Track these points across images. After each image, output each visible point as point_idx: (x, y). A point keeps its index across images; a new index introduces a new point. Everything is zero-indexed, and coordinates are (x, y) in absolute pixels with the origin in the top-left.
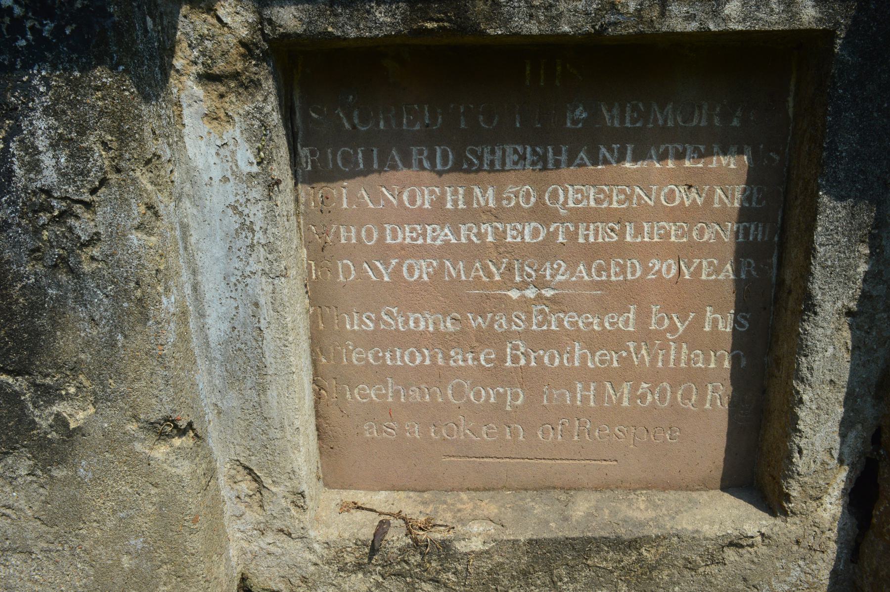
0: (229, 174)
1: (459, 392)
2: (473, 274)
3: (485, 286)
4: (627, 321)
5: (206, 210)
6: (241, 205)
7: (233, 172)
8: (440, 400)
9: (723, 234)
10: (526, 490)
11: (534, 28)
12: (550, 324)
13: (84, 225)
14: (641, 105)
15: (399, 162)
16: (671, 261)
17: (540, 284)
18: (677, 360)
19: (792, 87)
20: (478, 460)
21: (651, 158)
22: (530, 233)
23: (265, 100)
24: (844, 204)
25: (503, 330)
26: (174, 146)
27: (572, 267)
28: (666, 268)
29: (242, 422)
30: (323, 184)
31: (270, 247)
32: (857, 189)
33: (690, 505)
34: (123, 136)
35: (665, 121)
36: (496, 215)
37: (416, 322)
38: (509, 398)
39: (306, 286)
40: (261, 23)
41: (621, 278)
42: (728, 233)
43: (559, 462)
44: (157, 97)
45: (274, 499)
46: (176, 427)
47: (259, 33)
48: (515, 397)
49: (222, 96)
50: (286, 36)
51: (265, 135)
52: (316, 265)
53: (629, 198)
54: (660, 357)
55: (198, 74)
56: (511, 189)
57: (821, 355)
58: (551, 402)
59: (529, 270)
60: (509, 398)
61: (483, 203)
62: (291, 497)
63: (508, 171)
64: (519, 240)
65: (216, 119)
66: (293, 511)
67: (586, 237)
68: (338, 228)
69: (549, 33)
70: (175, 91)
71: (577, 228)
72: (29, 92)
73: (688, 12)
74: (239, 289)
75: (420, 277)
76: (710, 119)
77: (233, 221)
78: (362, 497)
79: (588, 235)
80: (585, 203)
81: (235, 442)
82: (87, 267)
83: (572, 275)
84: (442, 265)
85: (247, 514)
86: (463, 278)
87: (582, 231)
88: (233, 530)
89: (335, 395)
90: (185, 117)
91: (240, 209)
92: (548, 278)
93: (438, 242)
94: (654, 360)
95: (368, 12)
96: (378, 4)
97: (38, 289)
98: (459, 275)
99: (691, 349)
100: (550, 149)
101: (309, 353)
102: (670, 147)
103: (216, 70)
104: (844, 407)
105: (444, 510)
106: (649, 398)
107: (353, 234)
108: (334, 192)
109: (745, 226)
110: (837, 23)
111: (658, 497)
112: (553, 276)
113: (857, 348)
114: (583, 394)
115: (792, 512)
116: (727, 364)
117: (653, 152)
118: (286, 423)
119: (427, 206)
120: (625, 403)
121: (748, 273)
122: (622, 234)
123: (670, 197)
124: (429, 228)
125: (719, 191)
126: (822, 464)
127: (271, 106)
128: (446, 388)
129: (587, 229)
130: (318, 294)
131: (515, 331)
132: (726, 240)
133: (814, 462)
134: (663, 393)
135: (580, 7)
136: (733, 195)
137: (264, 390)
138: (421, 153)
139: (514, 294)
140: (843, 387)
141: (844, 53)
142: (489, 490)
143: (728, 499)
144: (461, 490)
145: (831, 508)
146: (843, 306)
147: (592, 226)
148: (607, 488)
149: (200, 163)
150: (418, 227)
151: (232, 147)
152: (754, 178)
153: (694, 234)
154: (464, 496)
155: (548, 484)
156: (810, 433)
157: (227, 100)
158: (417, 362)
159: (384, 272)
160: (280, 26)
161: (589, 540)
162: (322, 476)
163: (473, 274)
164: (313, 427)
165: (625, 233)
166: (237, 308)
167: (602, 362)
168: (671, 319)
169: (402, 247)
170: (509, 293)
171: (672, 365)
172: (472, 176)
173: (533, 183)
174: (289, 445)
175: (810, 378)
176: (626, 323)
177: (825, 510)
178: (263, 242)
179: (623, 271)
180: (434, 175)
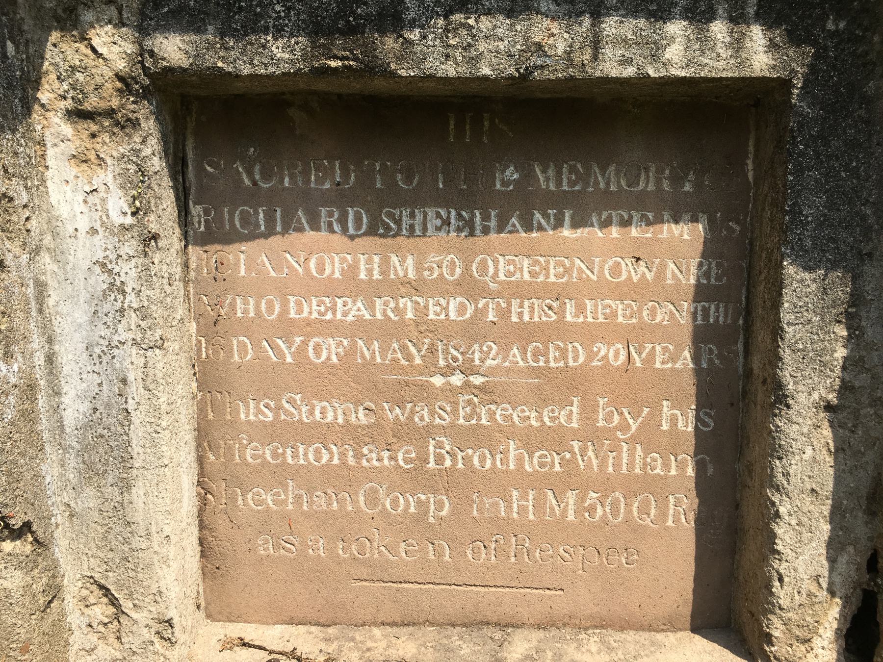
0: (97, 226)
1: (372, 499)
2: (389, 356)
3: (403, 371)
4: (570, 416)
5: (68, 267)
6: (111, 262)
7: (103, 224)
8: (350, 508)
9: (678, 316)
10: (454, 625)
11: (450, 70)
12: (479, 419)
14: (579, 166)
15: (305, 225)
16: (619, 346)
17: (468, 370)
18: (631, 464)
19: (751, 149)
20: (395, 585)
21: (592, 225)
22: (455, 308)
23: (144, 142)
24: (813, 276)
25: (425, 423)
26: (34, 190)
27: (505, 350)
29: (99, 528)
30: (218, 247)
31: (143, 312)
32: (828, 260)
33: (652, 649)
35: (608, 184)
36: (416, 288)
37: (323, 412)
38: (432, 507)
39: (194, 366)
40: (141, 55)
41: (562, 364)
42: (684, 314)
43: (493, 589)
44: (14, 131)
45: (134, 629)
46: (7, 526)
47: (139, 66)
48: (440, 506)
49: (93, 136)
50: (169, 70)
51: (143, 182)
52: (207, 342)
53: (568, 271)
54: (611, 461)
55: (67, 110)
56: (433, 258)
57: (797, 458)
58: (482, 513)
59: (455, 353)
60: (432, 507)
61: (401, 274)
62: (156, 627)
63: (429, 237)
64: (443, 317)
65: (85, 161)
66: (158, 645)
67: (520, 315)
68: (234, 299)
69: (468, 75)
70: (39, 127)
71: (509, 304)
73: (624, 56)
74: (104, 361)
75: (329, 358)
76: (658, 182)
78: (251, 632)
79: (522, 313)
80: (518, 275)
81: (90, 553)
83: (505, 359)
84: (354, 345)
85: (100, 648)
86: (379, 360)
87: (515, 308)
89: (224, 501)
90: (48, 158)
91: (110, 267)
92: (477, 362)
93: (350, 318)
95: (264, 47)
96: (275, 39)
98: (373, 357)
99: (647, 452)
100: (477, 213)
101: (193, 445)
102: (614, 214)
103: (87, 106)
104: (830, 523)
105: (350, 649)
106: (599, 511)
107: (251, 307)
108: (230, 256)
109: (704, 306)
110: (793, 71)
112: (482, 360)
113: (840, 450)
114: (520, 504)
115: (775, 657)
116: (690, 471)
117: (594, 219)
118: (153, 529)
119: (337, 275)
120: (571, 517)
121: (710, 361)
122: (561, 313)
123: (616, 270)
124: (340, 302)
125: (672, 266)
126: (808, 595)
128: (357, 494)
129: (521, 306)
130: (209, 379)
131: (439, 425)
132: (682, 322)
133: (799, 592)
134: (615, 506)
135: (502, 48)
136: (688, 270)
137: (129, 487)
138: (331, 214)
140: (827, 498)
141: (802, 104)
142: (408, 625)
143: (700, 642)
144: (374, 624)
146: (821, 398)
147: (526, 303)
148: (552, 626)
149: (63, 211)
150: (327, 300)
151: (102, 194)
152: (711, 251)
153: (645, 313)
154: (377, 632)
155: (480, 618)
156: (791, 555)
157: (99, 140)
158: (324, 461)
159: (286, 352)
160: (163, 59)
162: (203, 605)
163: (389, 356)
164: (195, 541)
165: (564, 312)
166: (100, 385)
167: (542, 465)
168: (621, 414)
169: (308, 323)
170: (431, 379)
171: (624, 471)
172: (389, 241)
173: (459, 251)
174: (156, 558)
175: (786, 486)
176: (569, 416)
177: (816, 656)
178: (135, 305)
180: (346, 240)
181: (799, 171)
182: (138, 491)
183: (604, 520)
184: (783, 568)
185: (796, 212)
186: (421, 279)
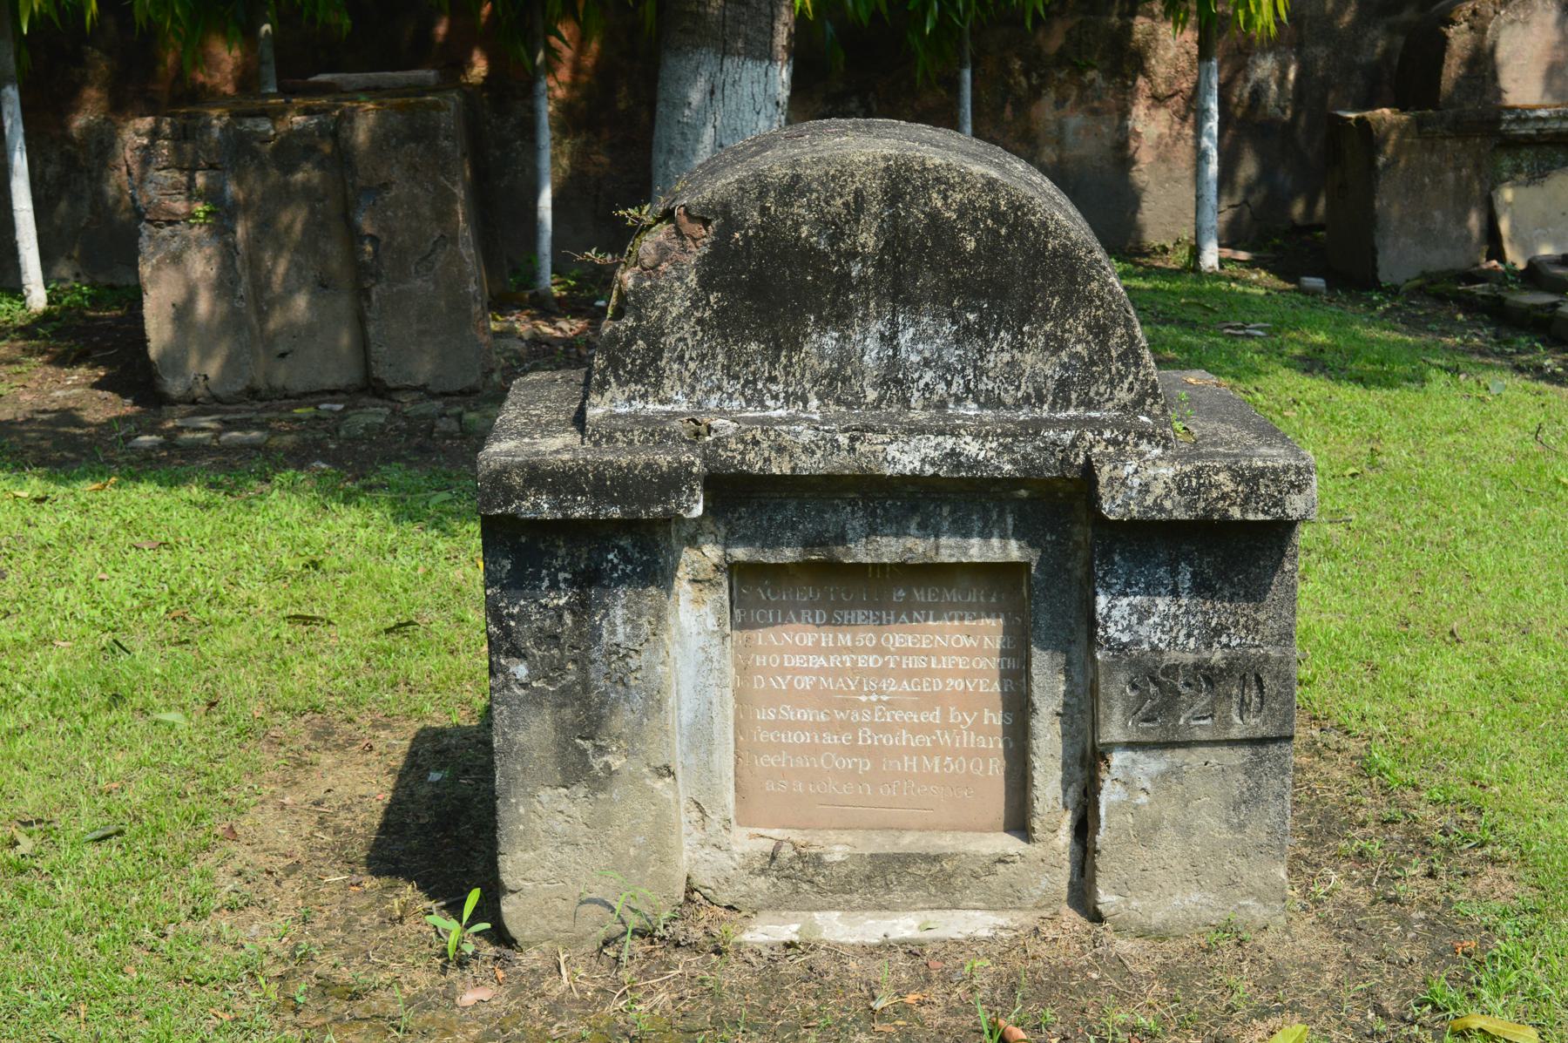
1: (828, 761)
3: (844, 693)
4: (935, 716)
9: (993, 663)
13: (633, 662)
17: (880, 692)
22: (872, 661)
27: (899, 683)
34: (659, 618)
36: (852, 650)
50: (737, 563)
72: (615, 597)
77: (701, 656)
82: (632, 683)
88: (685, 841)
94: (953, 742)
97: (606, 693)
99: (977, 735)
111: (959, 835)
114: (908, 763)
116: (1001, 746)
122: (929, 663)
127: (726, 597)
130: (741, 697)
134: (961, 764)
139: (863, 698)
145: (1064, 838)
149: (686, 625)
152: (1007, 631)
161: (909, 855)
179: (931, 684)
181: (1037, 604)
182: (716, 756)
183: (955, 772)
184: (1038, 793)
185: (1036, 622)
186: (854, 646)
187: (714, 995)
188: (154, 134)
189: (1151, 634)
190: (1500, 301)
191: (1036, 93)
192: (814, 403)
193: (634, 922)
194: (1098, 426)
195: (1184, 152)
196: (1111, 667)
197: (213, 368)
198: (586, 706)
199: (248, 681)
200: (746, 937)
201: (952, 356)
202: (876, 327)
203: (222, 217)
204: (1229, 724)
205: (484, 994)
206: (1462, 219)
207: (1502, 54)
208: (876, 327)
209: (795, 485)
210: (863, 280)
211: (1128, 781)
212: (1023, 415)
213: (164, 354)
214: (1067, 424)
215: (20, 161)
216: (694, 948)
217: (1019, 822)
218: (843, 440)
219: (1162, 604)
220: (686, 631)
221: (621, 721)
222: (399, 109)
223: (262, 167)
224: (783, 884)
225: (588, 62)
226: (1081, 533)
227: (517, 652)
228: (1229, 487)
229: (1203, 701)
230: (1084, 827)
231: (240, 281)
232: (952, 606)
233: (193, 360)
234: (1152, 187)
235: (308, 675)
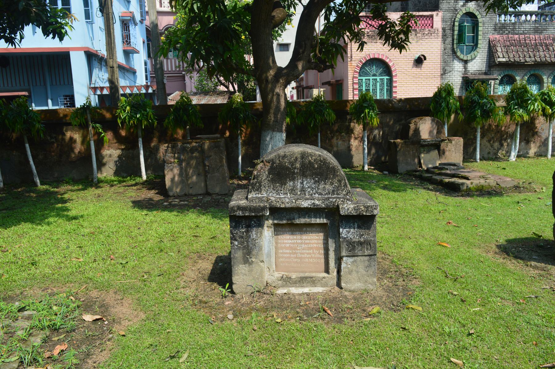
4: (311, 251)
9: (322, 242)
13: (256, 242)
22: (300, 241)
28: (315, 245)
36: (296, 239)
114: (307, 260)
130: (276, 248)
145: (335, 274)
152: (324, 236)
187: (272, 302)
188: (168, 147)
189: (350, 236)
190: (421, 176)
191: (333, 137)
192: (289, 194)
193: (257, 289)
194: (339, 198)
195: (361, 148)
196: (343, 242)
197: (178, 190)
198: (248, 250)
199: (186, 248)
200: (277, 292)
201: (313, 186)
202: (300, 181)
203: (180, 162)
204: (365, 252)
205: (229, 302)
206: (414, 160)
207: (420, 129)
208: (300, 181)
209: (285, 209)
210: (297, 173)
211: (347, 263)
212: (326, 196)
213: (169, 187)
214: (334, 198)
215: (142, 152)
216: (268, 294)
217: (327, 271)
218: (294, 201)
219: (352, 230)
220: (266, 236)
221: (254, 252)
222: (213, 142)
223: (188, 153)
224: (284, 283)
225: (248, 133)
226: (337, 218)
227: (236, 240)
228: (363, 209)
229: (360, 248)
230: (339, 272)
231: (183, 174)
232: (314, 231)
233: (174, 189)
234: (355, 155)
235: (197, 246)
